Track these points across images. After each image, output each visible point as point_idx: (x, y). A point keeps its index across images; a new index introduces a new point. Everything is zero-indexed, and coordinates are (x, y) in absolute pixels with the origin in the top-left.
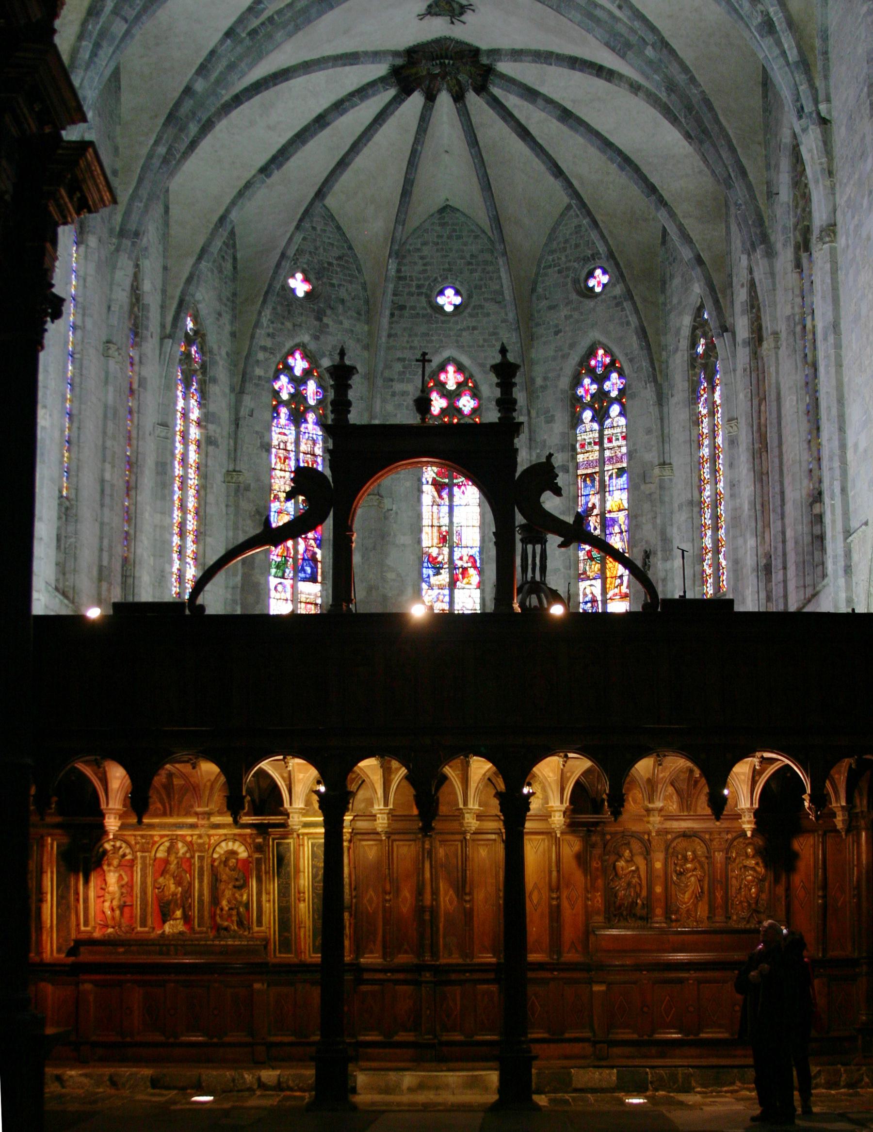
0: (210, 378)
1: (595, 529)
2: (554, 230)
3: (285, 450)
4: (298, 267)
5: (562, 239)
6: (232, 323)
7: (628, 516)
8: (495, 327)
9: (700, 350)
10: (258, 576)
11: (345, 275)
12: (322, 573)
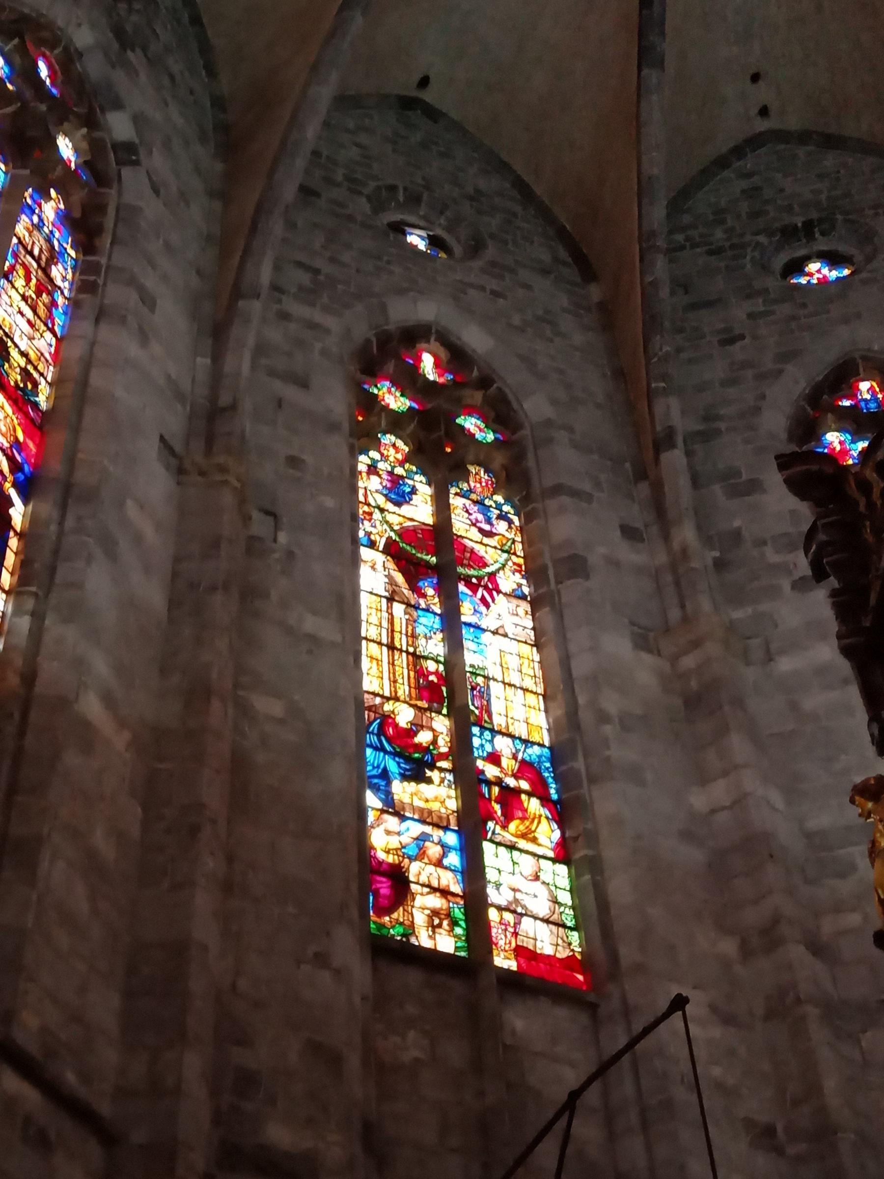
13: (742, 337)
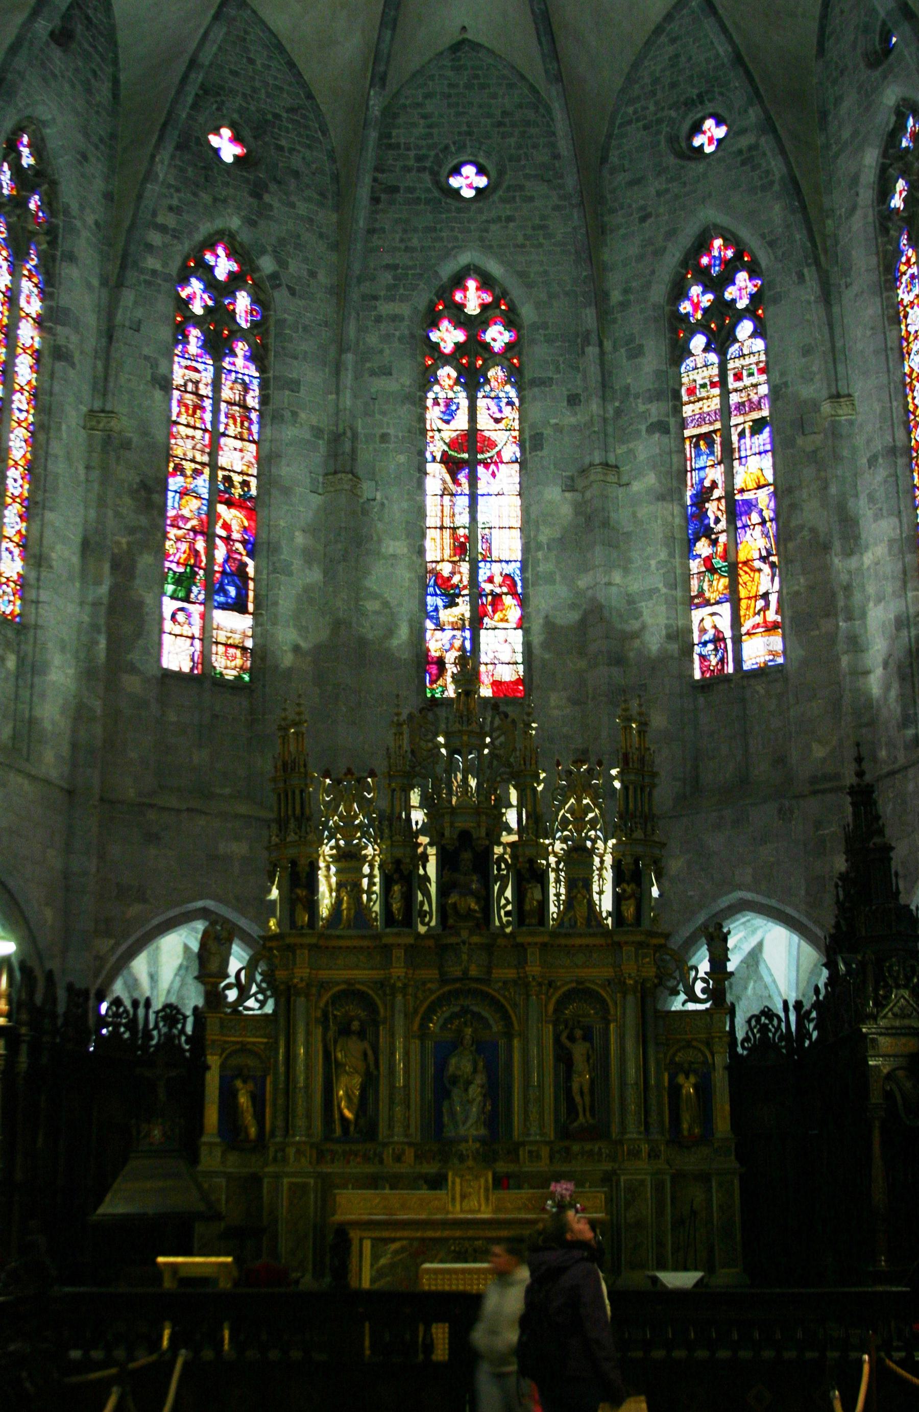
0: (63, 254)
1: (717, 520)
2: (635, 66)
3: (196, 393)
4: (223, 117)
5: (647, 80)
6: (107, 179)
7: (775, 494)
8: (543, 218)
9: (897, 202)
10: (141, 591)
11: (299, 135)
12: (255, 597)
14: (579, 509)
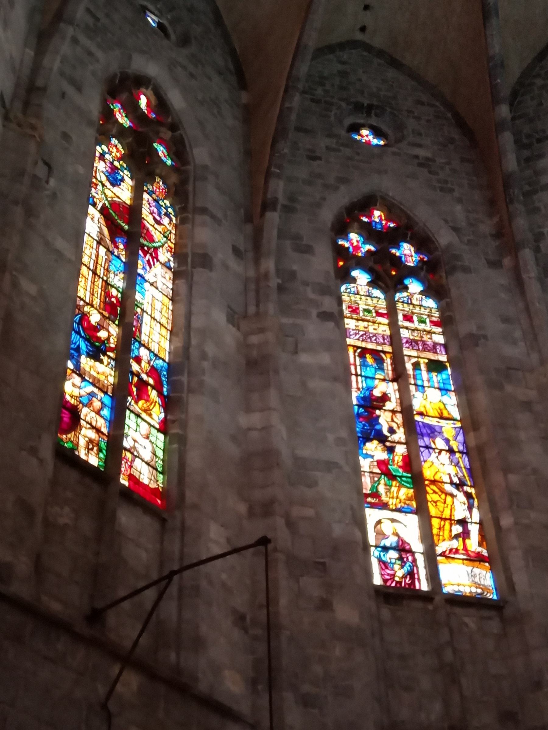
13: (320, 158)
14: (244, 346)
